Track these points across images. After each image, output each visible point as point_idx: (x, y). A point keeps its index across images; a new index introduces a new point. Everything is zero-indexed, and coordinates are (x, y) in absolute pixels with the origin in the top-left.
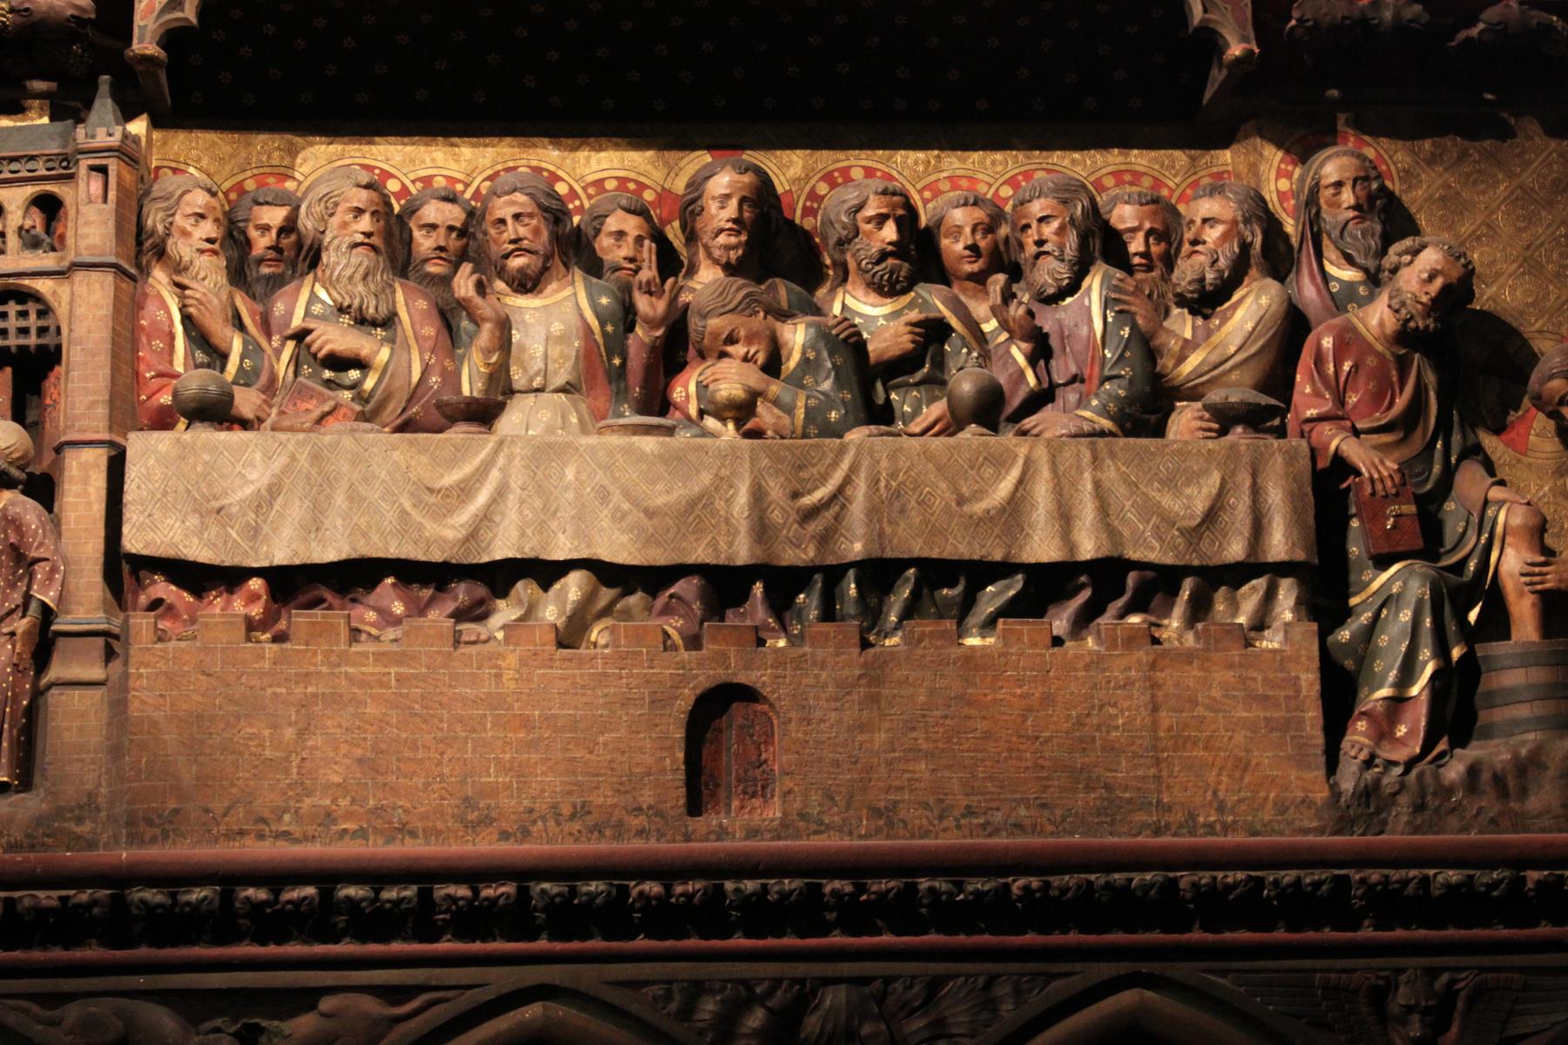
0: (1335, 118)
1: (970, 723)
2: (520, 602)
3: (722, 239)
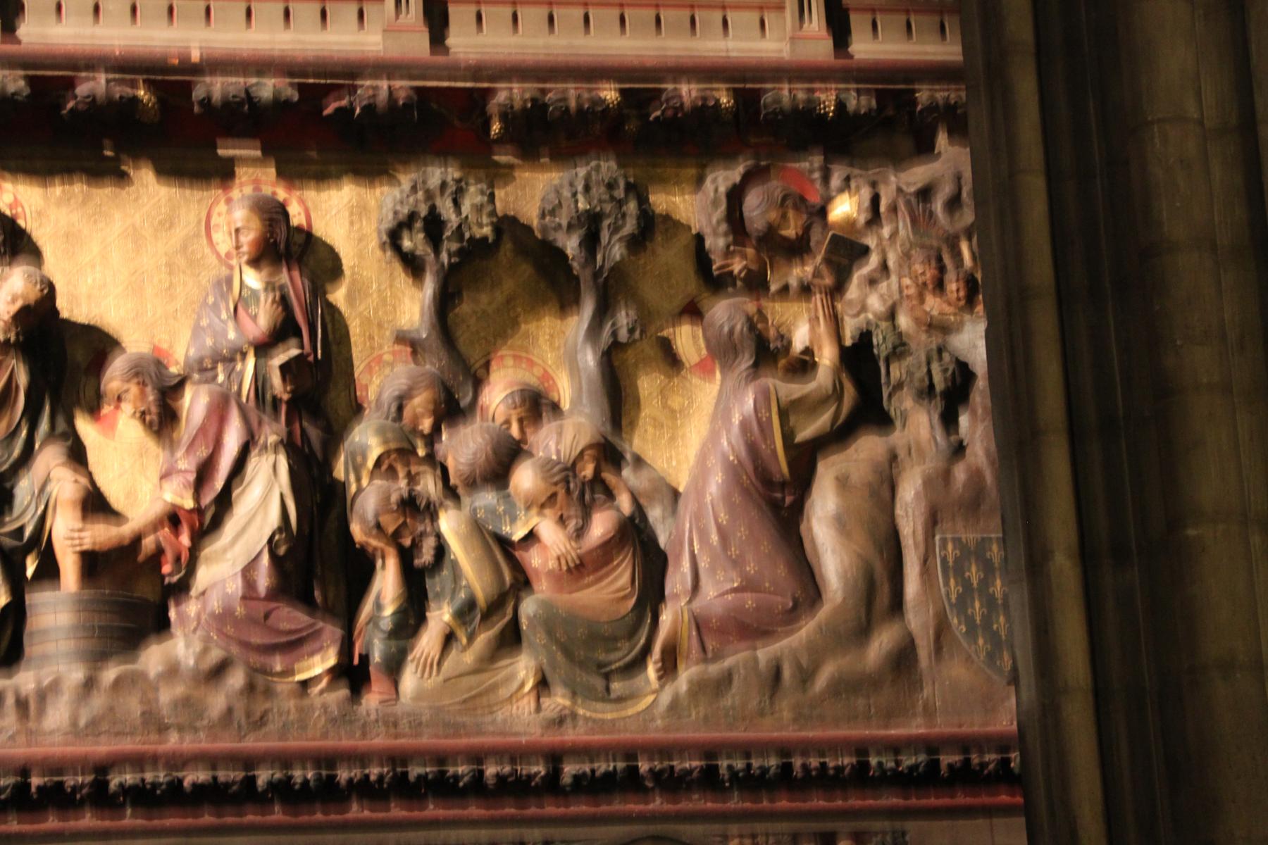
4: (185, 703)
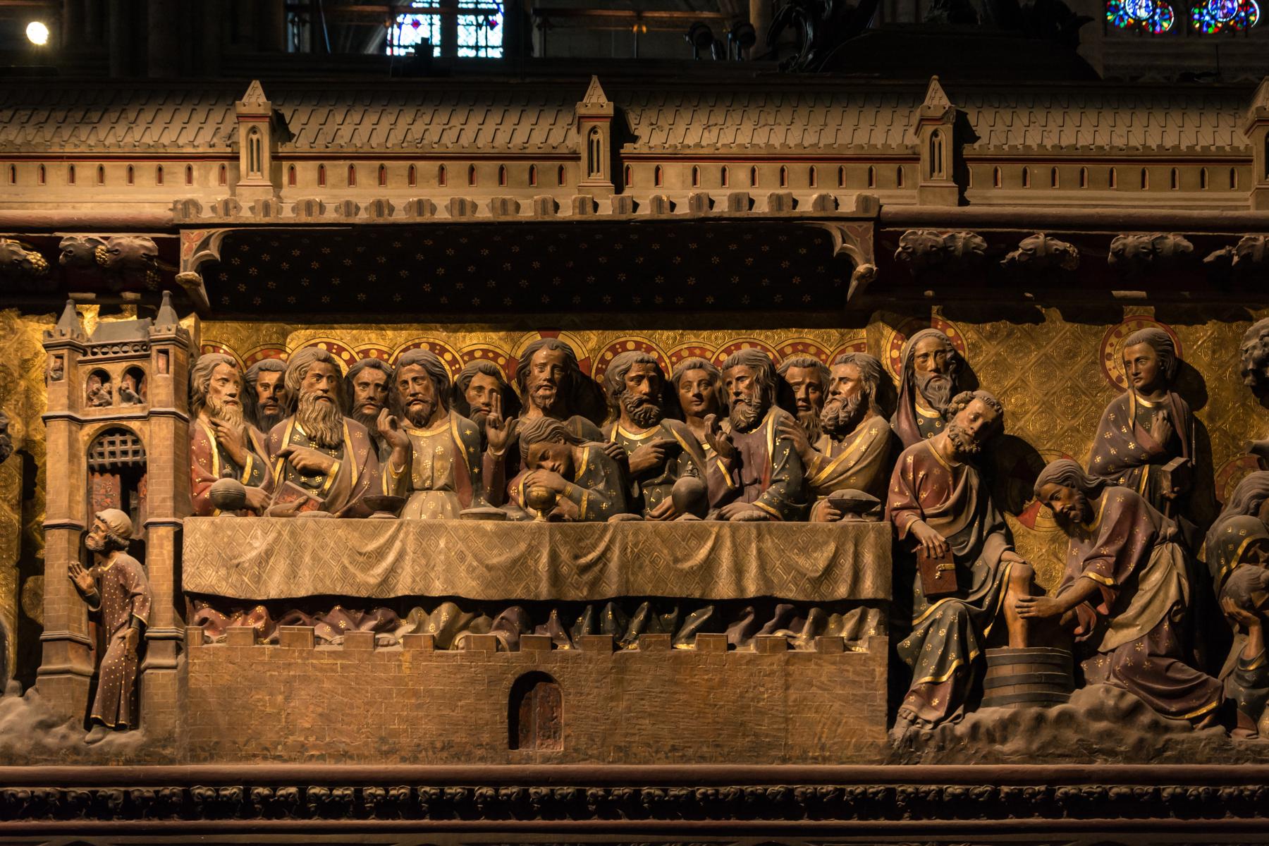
0: (930, 309)
1: (677, 696)
2: (413, 622)
3: (541, 392)
4: (1108, 734)
